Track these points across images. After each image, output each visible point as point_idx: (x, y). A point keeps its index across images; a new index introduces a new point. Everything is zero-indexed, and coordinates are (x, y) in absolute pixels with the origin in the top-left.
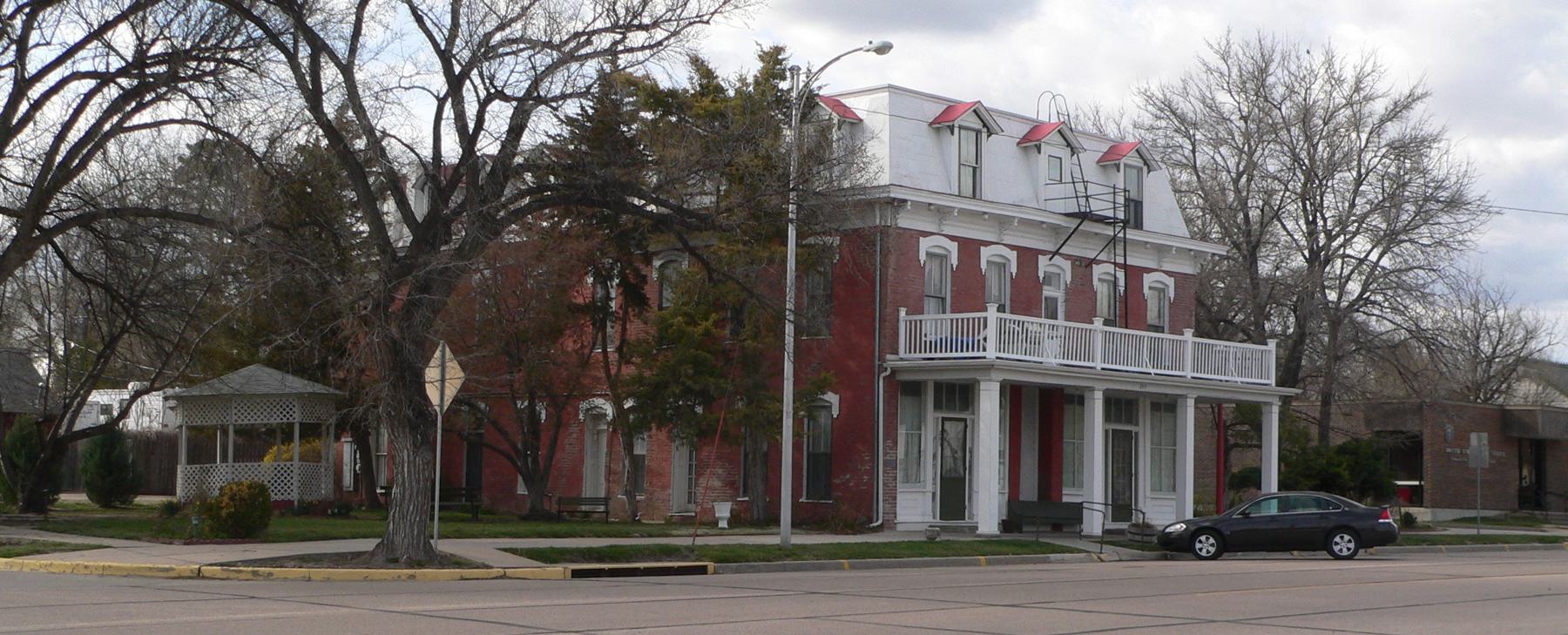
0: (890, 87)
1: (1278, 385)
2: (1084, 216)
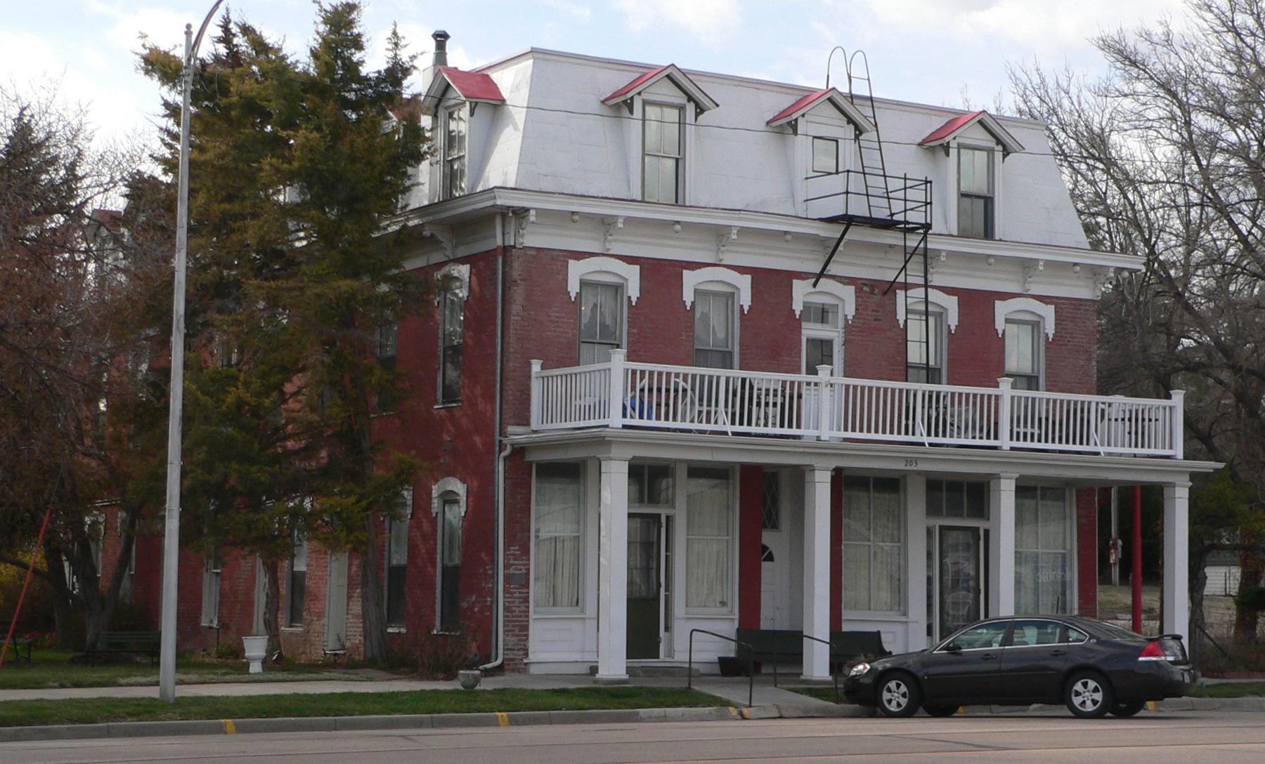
0: (533, 51)
1: (1186, 457)
2: (848, 220)
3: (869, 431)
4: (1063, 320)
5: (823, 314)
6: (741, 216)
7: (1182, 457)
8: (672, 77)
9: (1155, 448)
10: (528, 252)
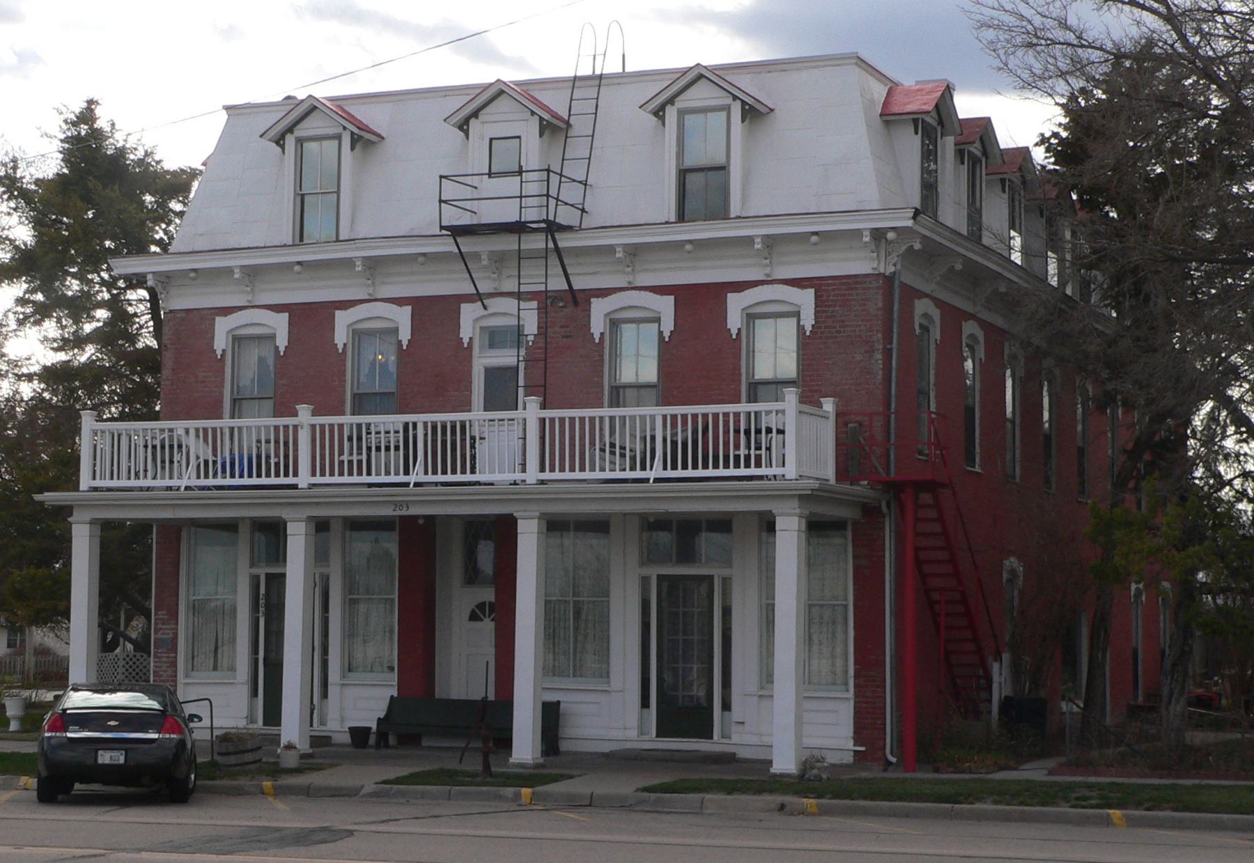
4: (830, 306)
6: (358, 245)
9: (118, 479)
10: (179, 315)
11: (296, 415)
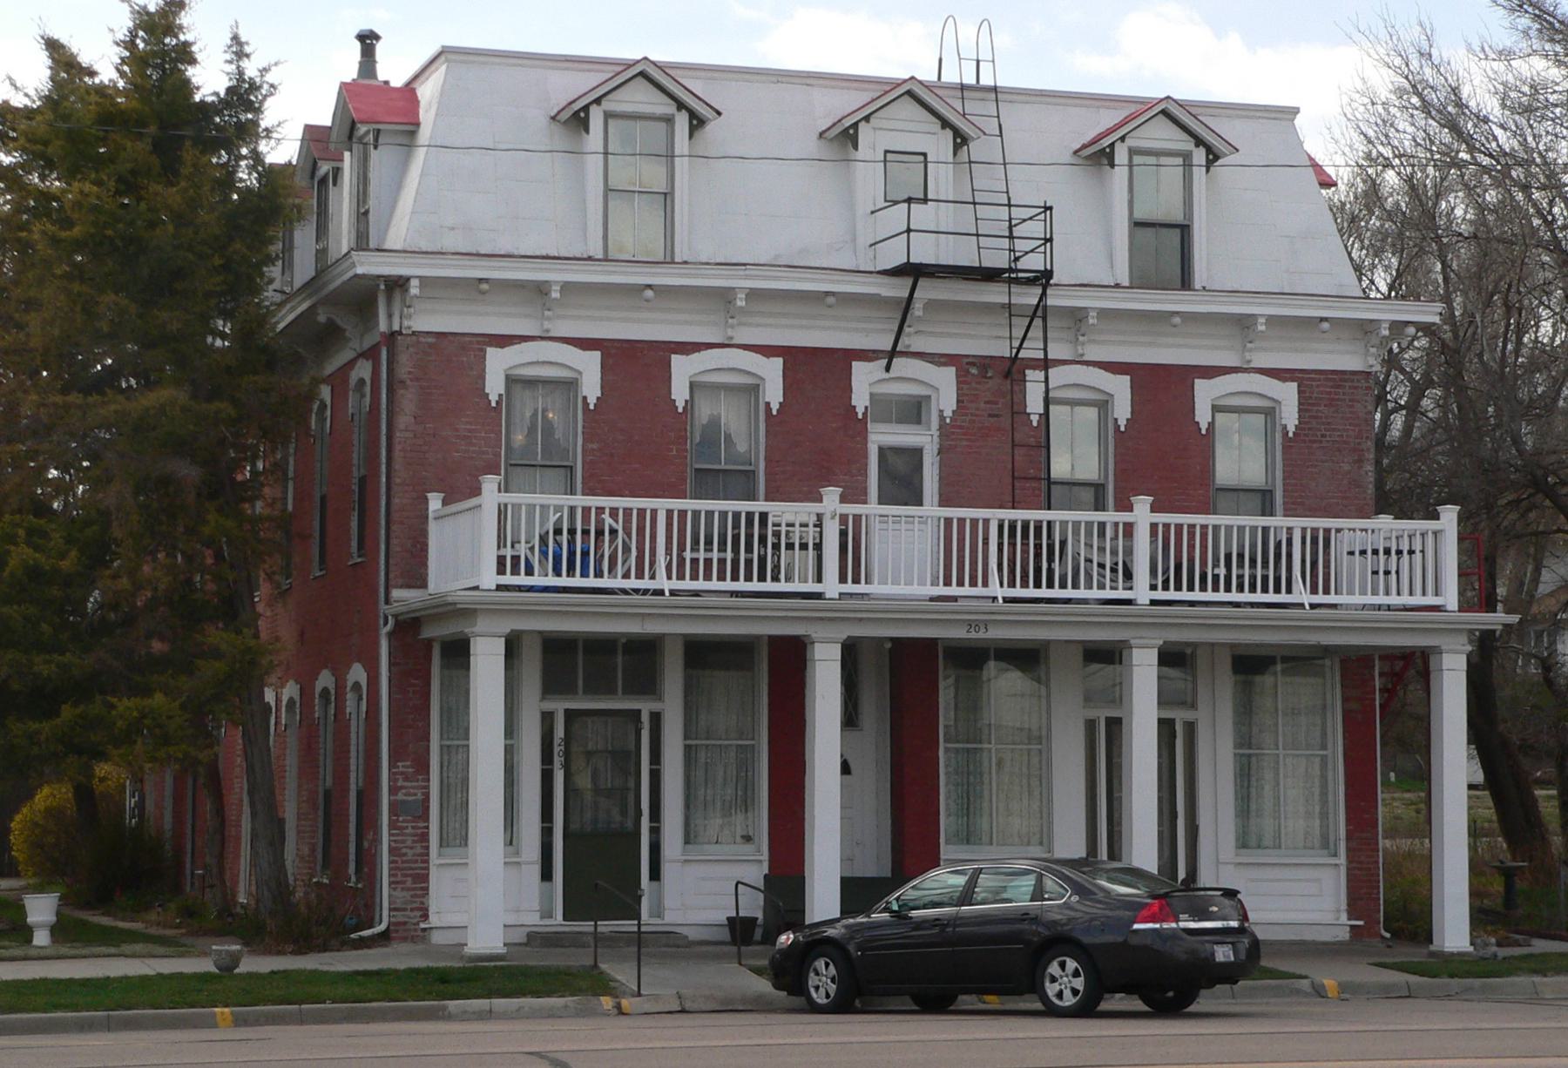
0: (444, 53)
2: (913, 272)
3: (735, 578)
4: (1313, 405)
5: (913, 410)
6: (747, 272)
7: (1456, 609)
8: (1169, 112)
10: (422, 339)
11: (1131, 510)
